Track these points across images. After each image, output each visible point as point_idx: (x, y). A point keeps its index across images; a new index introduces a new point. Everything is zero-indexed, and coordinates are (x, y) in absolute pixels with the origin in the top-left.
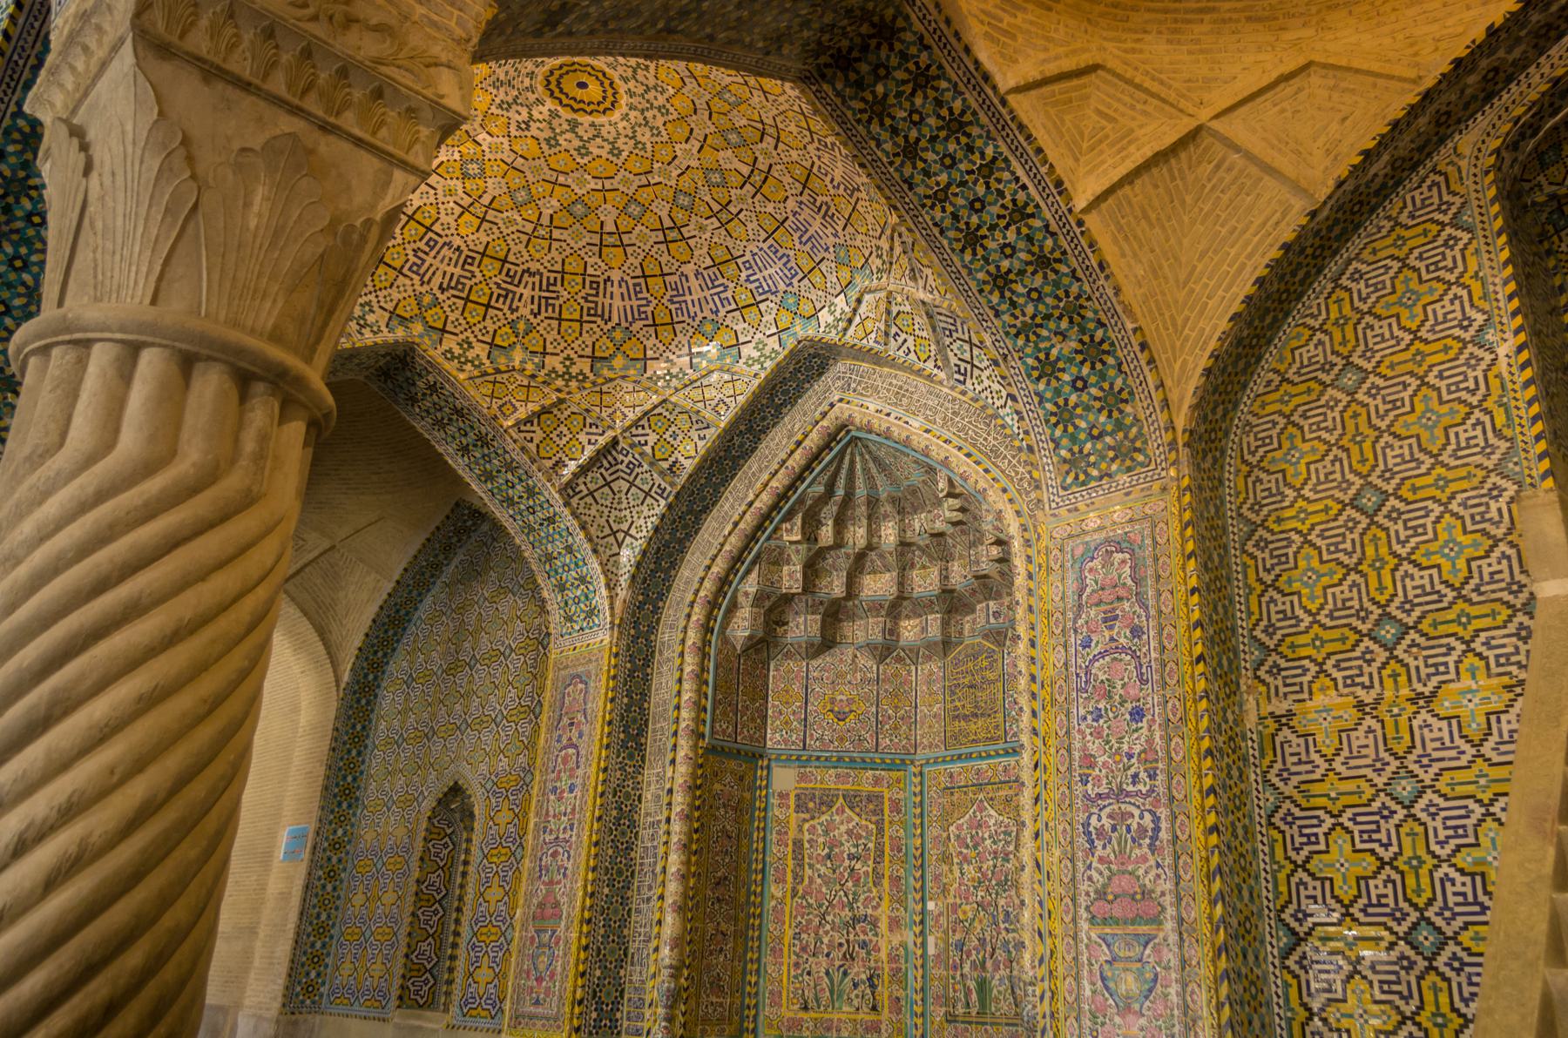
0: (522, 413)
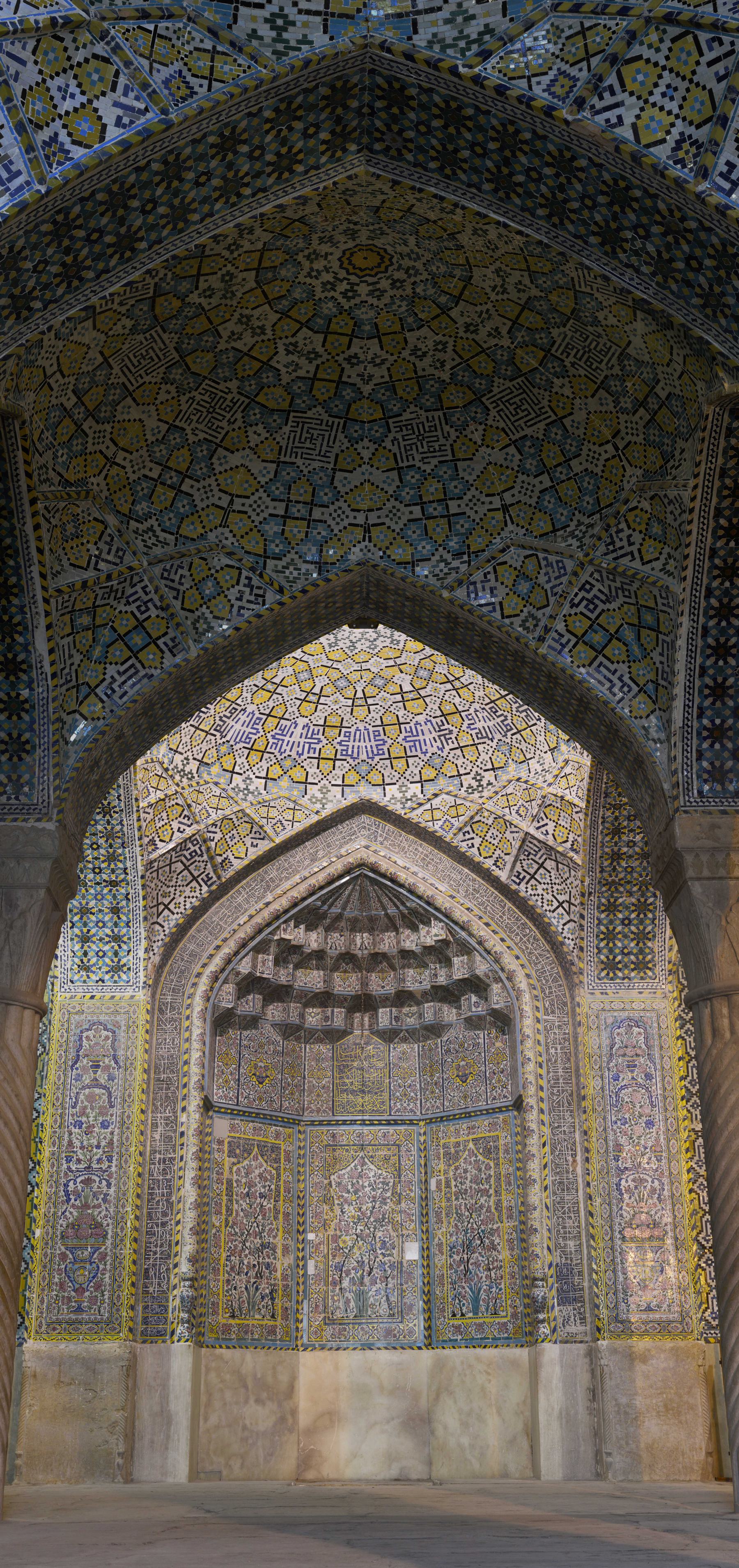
0: (152, 799)
